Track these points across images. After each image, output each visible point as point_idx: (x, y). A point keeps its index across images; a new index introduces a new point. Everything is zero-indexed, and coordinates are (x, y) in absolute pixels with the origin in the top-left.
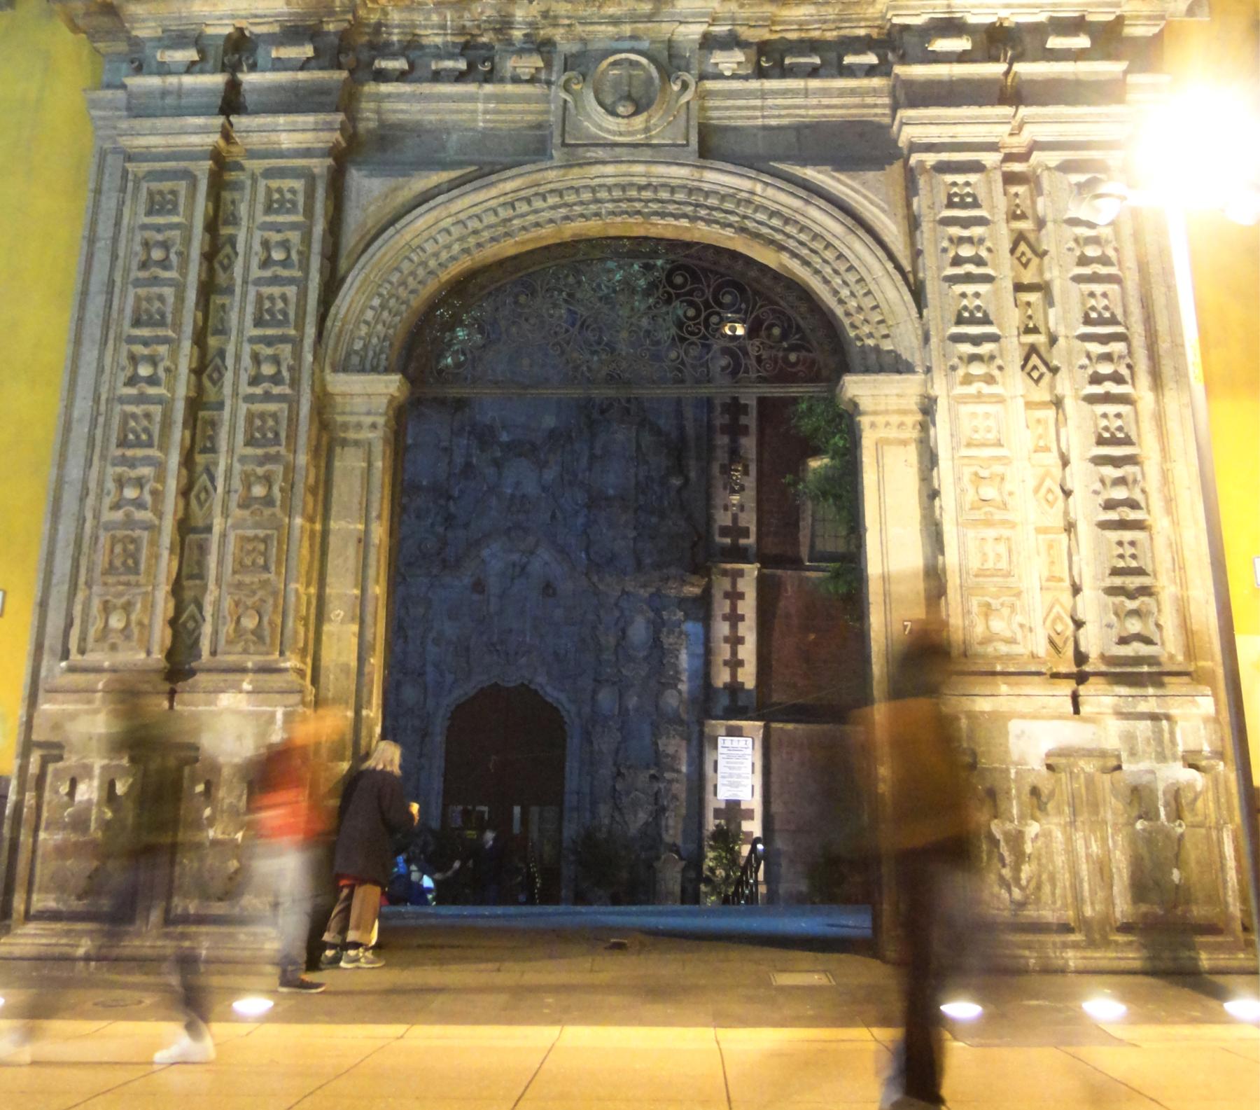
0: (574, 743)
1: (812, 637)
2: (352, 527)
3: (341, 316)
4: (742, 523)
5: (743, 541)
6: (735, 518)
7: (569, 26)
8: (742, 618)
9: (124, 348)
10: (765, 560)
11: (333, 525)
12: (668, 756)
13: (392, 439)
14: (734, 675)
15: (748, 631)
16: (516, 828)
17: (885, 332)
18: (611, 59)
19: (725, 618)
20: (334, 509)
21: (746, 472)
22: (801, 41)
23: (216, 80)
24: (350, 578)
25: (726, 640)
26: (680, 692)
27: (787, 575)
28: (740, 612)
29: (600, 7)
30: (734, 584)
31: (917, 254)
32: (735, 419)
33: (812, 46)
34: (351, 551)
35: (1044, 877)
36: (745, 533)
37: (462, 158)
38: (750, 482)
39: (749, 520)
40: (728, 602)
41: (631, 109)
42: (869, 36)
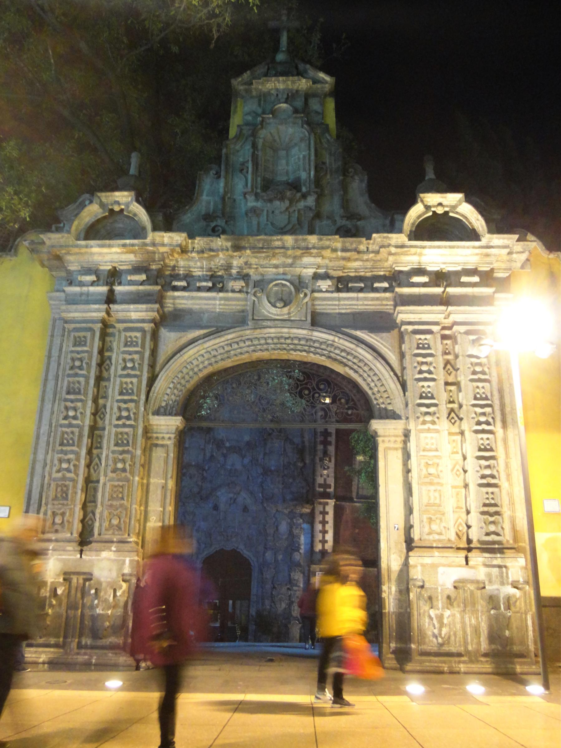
1: (357, 531)
2: (160, 481)
3: (157, 391)
4: (328, 482)
5: (328, 490)
6: (325, 480)
7: (257, 268)
8: (327, 522)
9: (63, 404)
10: (337, 498)
11: (152, 481)
12: (295, 580)
13: (178, 444)
14: (323, 546)
15: (330, 527)
16: (230, 610)
17: (389, 402)
18: (274, 283)
19: (320, 522)
20: (152, 475)
21: (330, 461)
22: (356, 277)
23: (104, 289)
24: (158, 504)
25: (320, 532)
26: (300, 553)
27: (346, 504)
28: (326, 520)
29: (270, 260)
30: (324, 508)
31: (403, 369)
32: (326, 438)
33: (360, 279)
34: (159, 492)
35: (452, 633)
37: (209, 324)
38: (332, 465)
39: (331, 481)
40: (321, 516)
41: (282, 305)
42: (385, 275)
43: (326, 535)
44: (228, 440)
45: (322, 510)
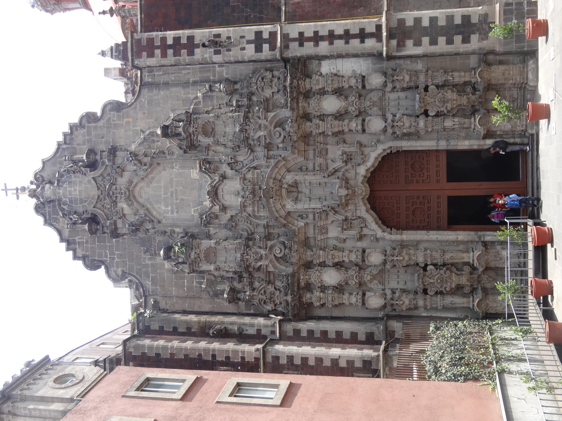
0: (407, 145)
19: (316, 45)
25: (331, 43)
28: (312, 35)
30: (294, 40)
36: (259, 34)
43: (336, 33)
44: (201, 203)
45: (297, 43)
